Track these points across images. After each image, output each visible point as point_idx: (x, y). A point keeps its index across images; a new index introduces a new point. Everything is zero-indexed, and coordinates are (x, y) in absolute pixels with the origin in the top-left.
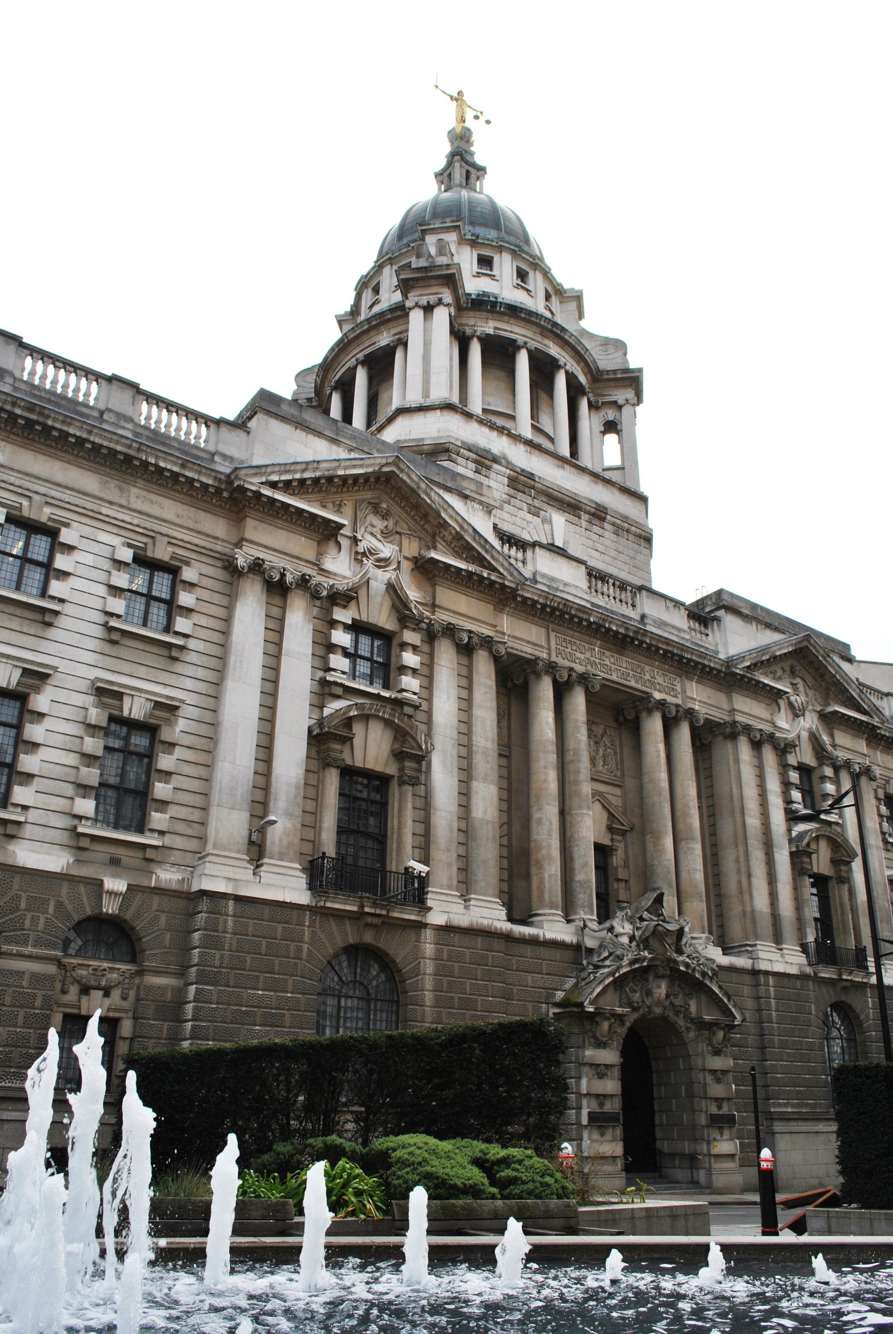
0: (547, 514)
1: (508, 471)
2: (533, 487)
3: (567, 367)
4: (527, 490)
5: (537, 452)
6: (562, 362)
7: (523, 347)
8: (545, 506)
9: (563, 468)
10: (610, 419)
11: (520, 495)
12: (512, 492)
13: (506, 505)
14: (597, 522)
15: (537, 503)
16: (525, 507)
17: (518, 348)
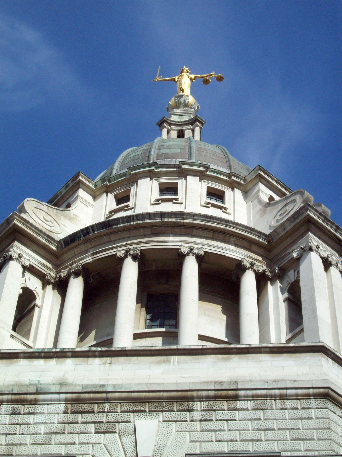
0: (130, 425)
1: (63, 396)
2: (107, 400)
3: (195, 251)
4: (96, 408)
5: (122, 359)
6: (184, 250)
7: (126, 256)
8: (125, 417)
9: (169, 361)
10: (293, 280)
11: (80, 418)
12: (70, 417)
13: (59, 438)
14: (225, 405)
15: (112, 417)
16: (92, 428)
17: (120, 261)
